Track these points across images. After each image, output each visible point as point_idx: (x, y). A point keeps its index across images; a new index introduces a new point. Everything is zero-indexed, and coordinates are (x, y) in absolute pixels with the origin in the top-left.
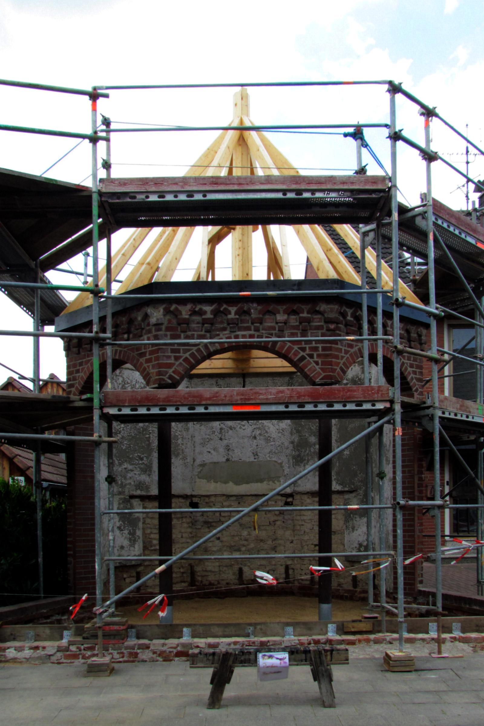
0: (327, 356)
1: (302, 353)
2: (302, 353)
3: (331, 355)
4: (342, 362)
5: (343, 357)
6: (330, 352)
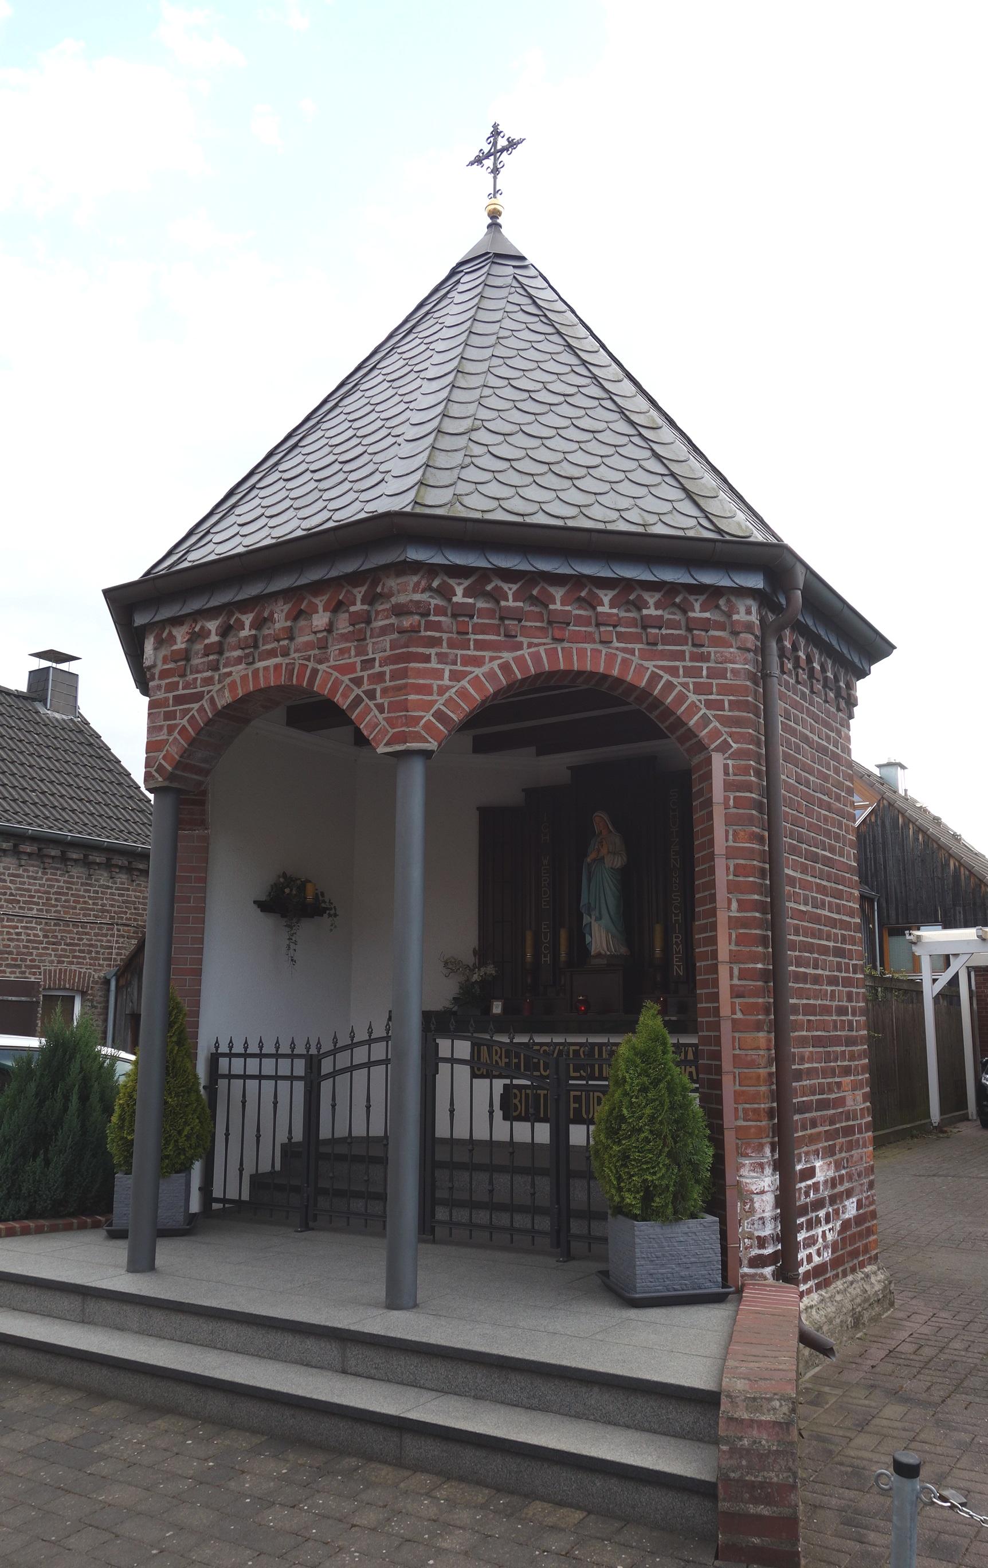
0: (399, 689)
1: (357, 691)
2: (357, 691)
3: (406, 685)
4: (442, 700)
5: (442, 691)
6: (404, 681)
